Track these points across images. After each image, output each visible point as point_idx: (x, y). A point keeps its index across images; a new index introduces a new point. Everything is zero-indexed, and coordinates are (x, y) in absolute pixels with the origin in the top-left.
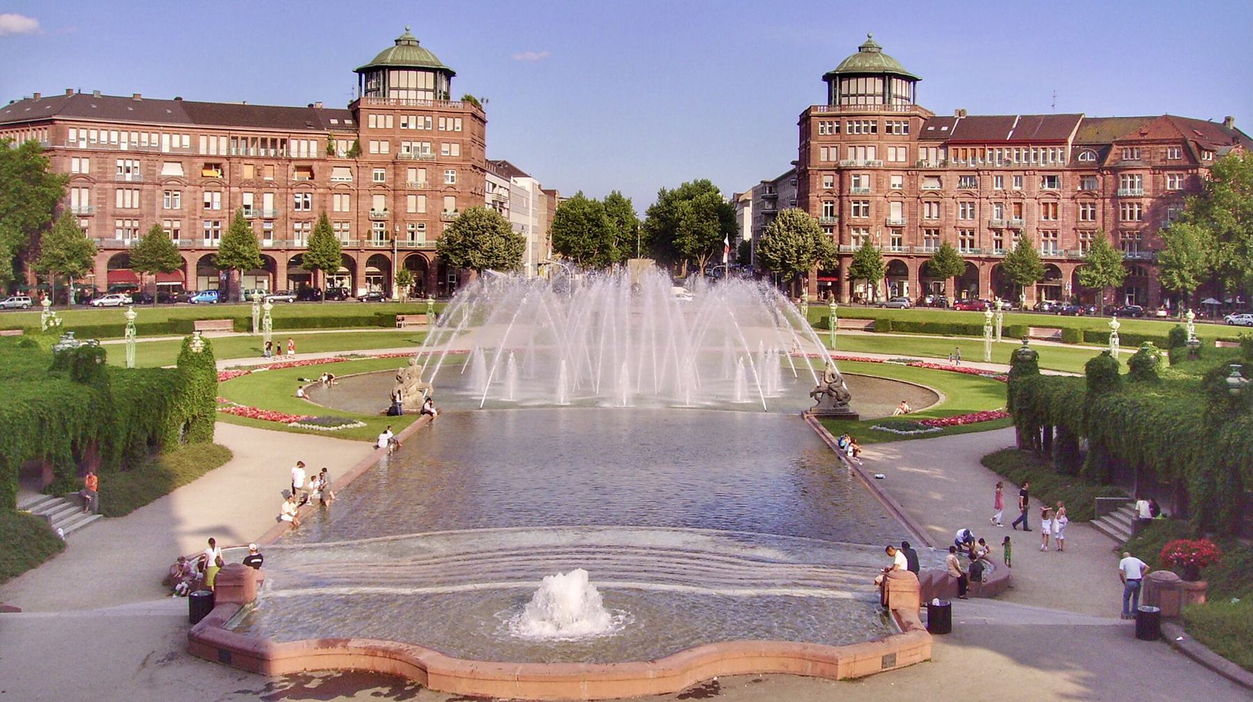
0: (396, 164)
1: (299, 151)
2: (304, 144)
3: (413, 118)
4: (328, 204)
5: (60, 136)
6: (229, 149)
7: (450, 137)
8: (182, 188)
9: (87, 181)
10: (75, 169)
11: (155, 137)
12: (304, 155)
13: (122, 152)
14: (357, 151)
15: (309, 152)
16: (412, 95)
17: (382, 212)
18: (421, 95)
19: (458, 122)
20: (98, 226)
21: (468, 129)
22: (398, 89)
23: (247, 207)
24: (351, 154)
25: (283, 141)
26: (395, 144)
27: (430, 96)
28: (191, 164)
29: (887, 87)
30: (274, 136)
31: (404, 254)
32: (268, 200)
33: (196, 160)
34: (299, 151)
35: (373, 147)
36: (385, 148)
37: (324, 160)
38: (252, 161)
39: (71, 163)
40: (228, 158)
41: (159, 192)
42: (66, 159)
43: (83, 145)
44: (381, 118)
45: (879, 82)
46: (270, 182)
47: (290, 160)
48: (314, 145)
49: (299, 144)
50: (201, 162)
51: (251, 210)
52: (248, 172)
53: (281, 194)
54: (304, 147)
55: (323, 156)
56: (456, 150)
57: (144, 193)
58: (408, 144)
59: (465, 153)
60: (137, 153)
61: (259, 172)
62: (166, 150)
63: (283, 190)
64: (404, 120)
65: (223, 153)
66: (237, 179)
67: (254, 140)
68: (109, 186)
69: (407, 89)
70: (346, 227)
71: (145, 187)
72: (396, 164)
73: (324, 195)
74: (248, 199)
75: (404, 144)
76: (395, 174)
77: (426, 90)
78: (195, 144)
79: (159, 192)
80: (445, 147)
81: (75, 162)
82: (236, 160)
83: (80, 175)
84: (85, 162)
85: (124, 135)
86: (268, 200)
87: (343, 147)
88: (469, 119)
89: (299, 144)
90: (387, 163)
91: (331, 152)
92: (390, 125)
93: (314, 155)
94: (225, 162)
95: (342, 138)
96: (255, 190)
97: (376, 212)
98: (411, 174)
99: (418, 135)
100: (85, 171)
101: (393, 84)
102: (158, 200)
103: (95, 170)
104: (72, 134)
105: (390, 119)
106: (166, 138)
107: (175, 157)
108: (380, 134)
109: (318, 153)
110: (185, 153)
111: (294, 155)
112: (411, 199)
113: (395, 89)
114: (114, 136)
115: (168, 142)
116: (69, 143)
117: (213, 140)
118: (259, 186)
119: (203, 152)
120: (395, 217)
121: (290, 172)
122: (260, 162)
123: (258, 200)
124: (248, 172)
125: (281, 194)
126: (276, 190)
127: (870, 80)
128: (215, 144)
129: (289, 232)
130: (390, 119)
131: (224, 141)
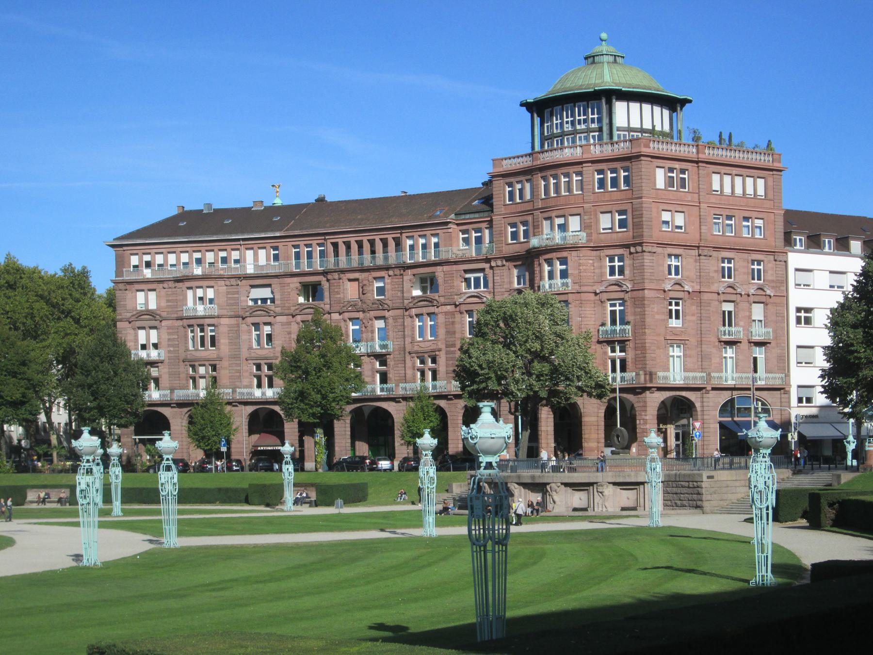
9: (150, 318)
20: (170, 374)
28: (282, 285)
38: (356, 275)
40: (325, 273)
41: (244, 327)
42: (129, 294)
53: (395, 318)
66: (339, 302)
73: (452, 314)
79: (244, 327)
81: (140, 296)
82: (336, 276)
84: (152, 296)
96: (361, 315)
100: (153, 306)
102: (244, 337)
103: (164, 304)
115: (255, 259)
121: (407, 285)
124: (351, 291)
125: (395, 318)
129: (409, 372)
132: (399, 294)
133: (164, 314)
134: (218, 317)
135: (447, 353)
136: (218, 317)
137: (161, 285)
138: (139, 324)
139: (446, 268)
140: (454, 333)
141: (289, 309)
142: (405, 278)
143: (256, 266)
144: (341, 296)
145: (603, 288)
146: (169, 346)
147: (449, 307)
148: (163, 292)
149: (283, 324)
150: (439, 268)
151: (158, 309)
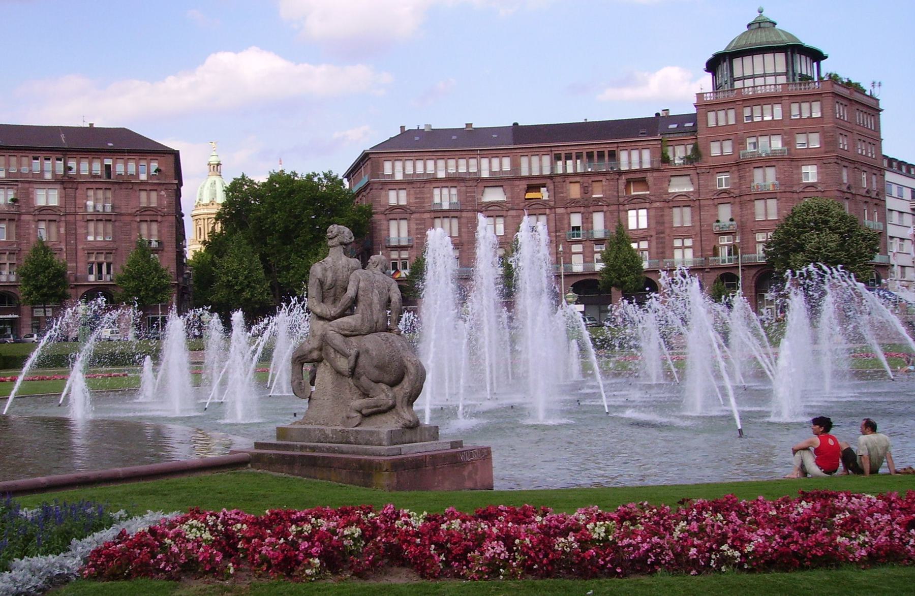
0: (740, 165)
1: (630, 163)
2: (635, 154)
3: (757, 109)
4: (666, 218)
5: (377, 169)
6: (552, 168)
7: (808, 125)
8: (504, 213)
10: (393, 201)
11: (473, 162)
12: (635, 167)
13: (441, 180)
14: (696, 157)
15: (641, 162)
16: (759, 81)
17: (728, 223)
18: (770, 80)
19: (816, 106)
21: (828, 112)
22: (743, 78)
23: (578, 228)
24: (688, 159)
25: (613, 155)
26: (739, 143)
27: (782, 80)
29: (790, 64)
30: (602, 148)
31: (754, 272)
32: (598, 221)
33: (517, 183)
34: (630, 163)
35: (715, 150)
36: (728, 149)
37: (658, 170)
38: (578, 179)
39: (388, 196)
40: (552, 177)
42: (383, 193)
43: (399, 177)
44: (721, 114)
45: (781, 58)
46: (598, 199)
47: (620, 173)
48: (646, 154)
49: (630, 155)
50: (523, 185)
51: (581, 232)
52: (575, 191)
53: (611, 212)
54: (633, 159)
55: (656, 166)
56: (815, 142)
57: (463, 220)
58: (753, 140)
59: (828, 142)
60: (452, 180)
61: (585, 190)
62: (485, 174)
63: (615, 208)
64: (747, 112)
65: (547, 172)
67: (601, 155)
68: (427, 216)
69: (753, 77)
70: (688, 242)
71: (464, 214)
72: (740, 165)
73: (662, 209)
74: (576, 220)
75: (749, 140)
76: (740, 177)
77: (776, 75)
78: (516, 165)
80: (800, 139)
83: (398, 207)
84: (403, 194)
85: (441, 163)
86: (598, 221)
87: (679, 154)
88: (829, 101)
89: (630, 155)
90: (730, 165)
91: (665, 160)
92: (732, 121)
93: (646, 166)
94: (549, 181)
95: (680, 143)
96: (582, 209)
97: (721, 224)
98: (758, 175)
99: (769, 129)
100: (403, 202)
101: (737, 73)
103: (412, 200)
104: (387, 168)
105: (731, 113)
106: (485, 162)
107: (495, 181)
108: (721, 134)
109: (652, 162)
110: (506, 176)
111: (624, 168)
112: (759, 205)
113: (739, 79)
114: (430, 164)
115: (486, 167)
116: (385, 176)
117: (535, 159)
118: (587, 206)
119: (525, 172)
120: (742, 228)
122: (586, 179)
123: (588, 220)
124: (575, 191)
125: (611, 212)
126: (605, 208)
127: (769, 57)
128: (536, 165)
130: (731, 113)
131: (546, 160)
132: (615, 193)
133: (413, 208)
134: (461, 211)
135: (657, 238)
136: (461, 211)
137: (410, 186)
138: (391, 216)
139: (655, 174)
140: (663, 223)
141: (518, 204)
142: (620, 181)
143: (491, 172)
144: (564, 195)
145: (801, 190)
146: (417, 234)
147: (658, 204)
148: (412, 192)
149: (513, 217)
150: (649, 174)
151: (409, 203)
